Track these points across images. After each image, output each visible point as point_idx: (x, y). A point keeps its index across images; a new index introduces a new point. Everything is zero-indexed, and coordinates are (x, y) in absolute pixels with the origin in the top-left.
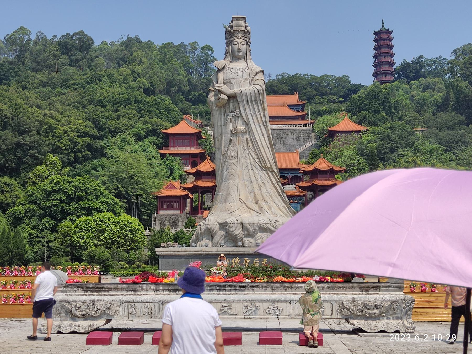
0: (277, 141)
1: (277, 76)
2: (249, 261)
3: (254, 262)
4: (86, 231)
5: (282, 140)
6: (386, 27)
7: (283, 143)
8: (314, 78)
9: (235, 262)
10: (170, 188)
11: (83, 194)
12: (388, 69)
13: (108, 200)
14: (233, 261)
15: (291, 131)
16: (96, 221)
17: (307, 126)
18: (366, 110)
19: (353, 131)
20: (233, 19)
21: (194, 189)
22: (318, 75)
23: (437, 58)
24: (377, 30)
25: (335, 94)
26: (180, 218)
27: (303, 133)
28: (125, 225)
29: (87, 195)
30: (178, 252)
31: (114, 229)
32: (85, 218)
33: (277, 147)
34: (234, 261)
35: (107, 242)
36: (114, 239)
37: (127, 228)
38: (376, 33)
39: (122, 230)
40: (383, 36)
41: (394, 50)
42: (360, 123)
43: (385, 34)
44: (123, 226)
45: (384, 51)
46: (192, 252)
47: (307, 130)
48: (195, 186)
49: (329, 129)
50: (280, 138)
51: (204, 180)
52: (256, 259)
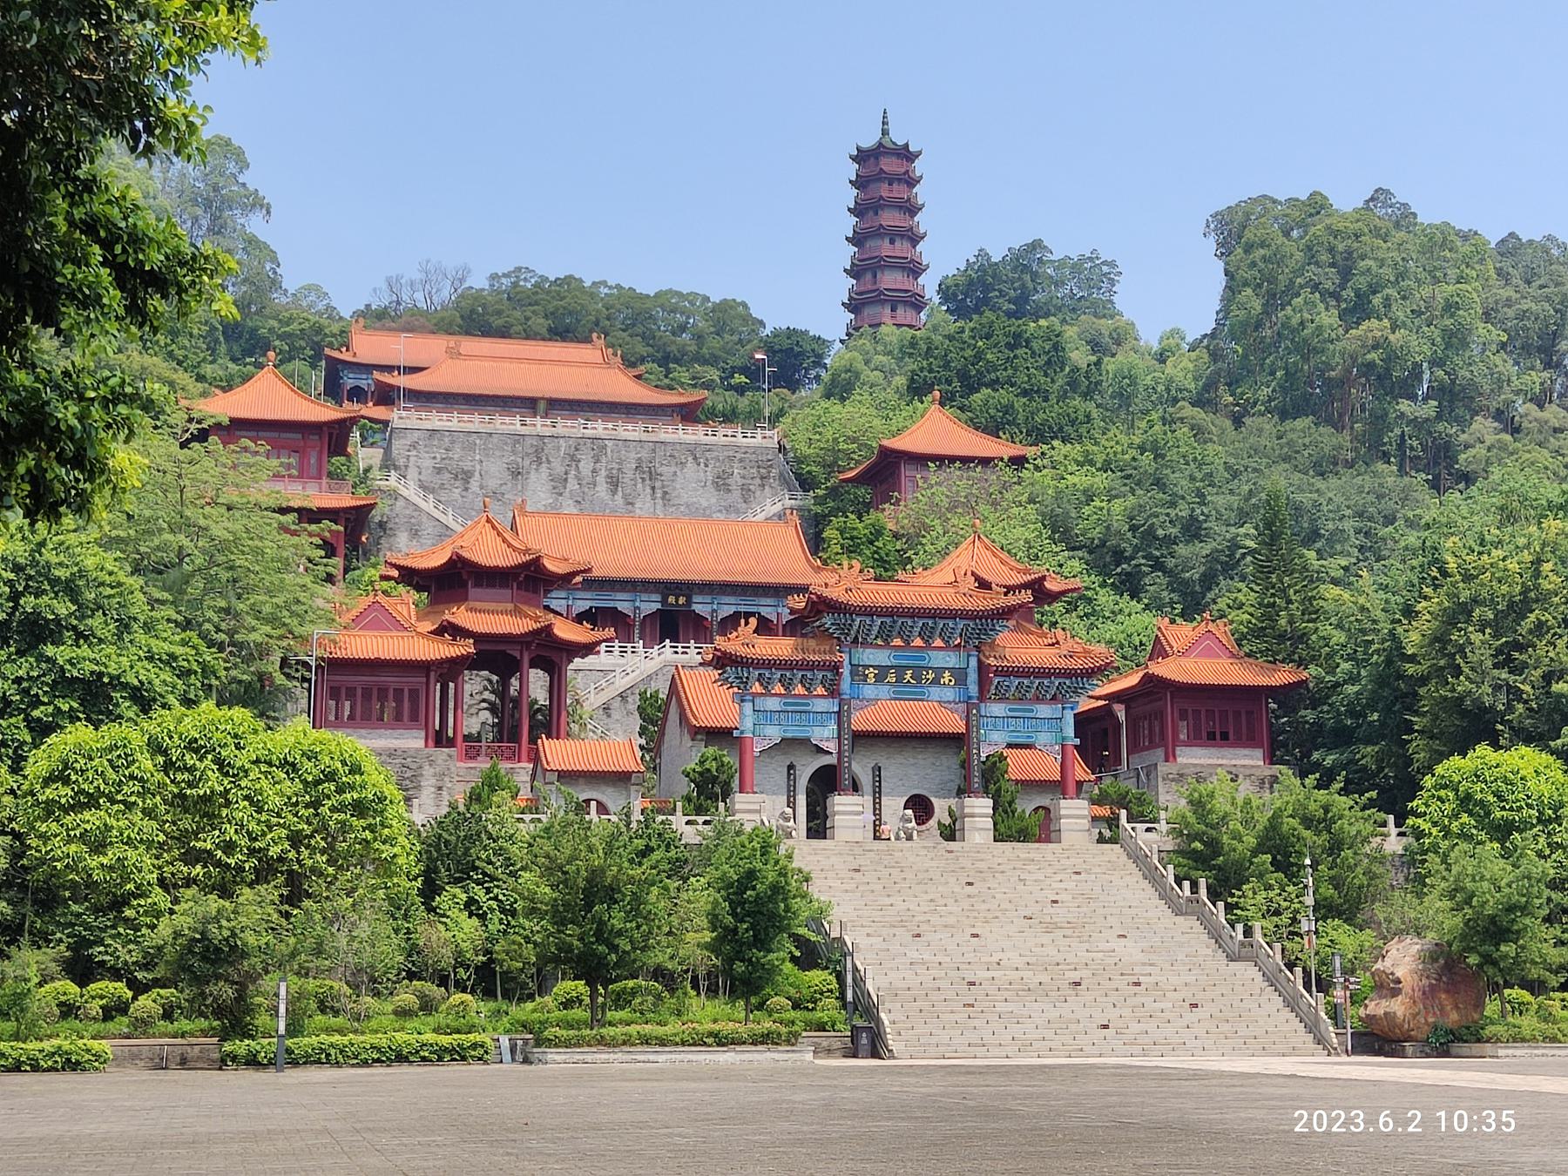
0: (640, 485)
1: (494, 277)
4: (113, 802)
5: (658, 484)
6: (898, 137)
7: (663, 498)
8: (629, 297)
10: (375, 625)
11: (64, 608)
12: (898, 287)
13: (179, 650)
15: (694, 451)
16: (165, 753)
17: (759, 436)
18: (993, 385)
19: (976, 458)
22: (647, 287)
23: (1083, 259)
24: (869, 140)
25: (712, 361)
26: (428, 771)
27: (741, 461)
28: (330, 776)
29: (83, 611)
31: (275, 801)
32: (78, 735)
33: (638, 511)
35: (240, 869)
36: (274, 851)
37: (340, 791)
38: (862, 156)
39: (315, 804)
40: (889, 165)
41: (922, 221)
42: (993, 429)
43: (894, 159)
44: (318, 782)
45: (890, 218)
47: (756, 450)
49: (886, 443)
50: (653, 475)
51: (478, 605)
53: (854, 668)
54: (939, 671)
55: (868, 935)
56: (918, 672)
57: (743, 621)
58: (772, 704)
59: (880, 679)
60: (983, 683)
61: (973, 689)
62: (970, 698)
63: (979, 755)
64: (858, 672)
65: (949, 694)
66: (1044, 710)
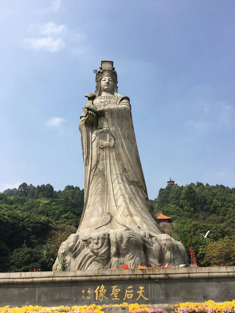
2: (119, 290)
3: (127, 292)
6: (172, 180)
9: (99, 293)
14: (96, 291)
20: (103, 62)
24: (169, 181)
30: (9, 278)
34: (98, 291)
46: (40, 277)
52: (129, 288)
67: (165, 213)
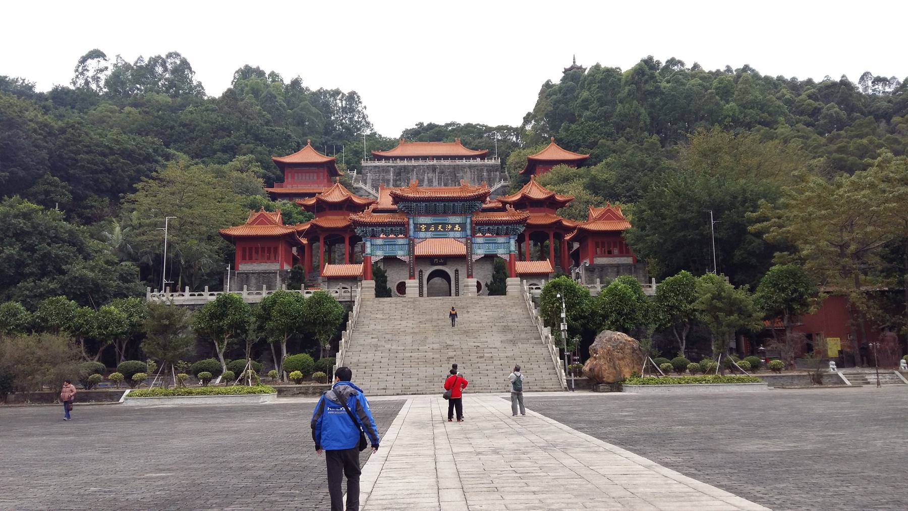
6: (578, 64)
15: (470, 167)
21: (314, 233)
24: (568, 67)
48: (314, 227)
49: (530, 157)
53: (415, 225)
54: (454, 225)
55: (372, 338)
56: (444, 225)
57: (366, 208)
58: (379, 242)
59: (427, 230)
60: (472, 229)
61: (469, 232)
62: (467, 236)
63: (471, 260)
64: (417, 228)
65: (458, 234)
66: (501, 240)
67: (566, 145)
